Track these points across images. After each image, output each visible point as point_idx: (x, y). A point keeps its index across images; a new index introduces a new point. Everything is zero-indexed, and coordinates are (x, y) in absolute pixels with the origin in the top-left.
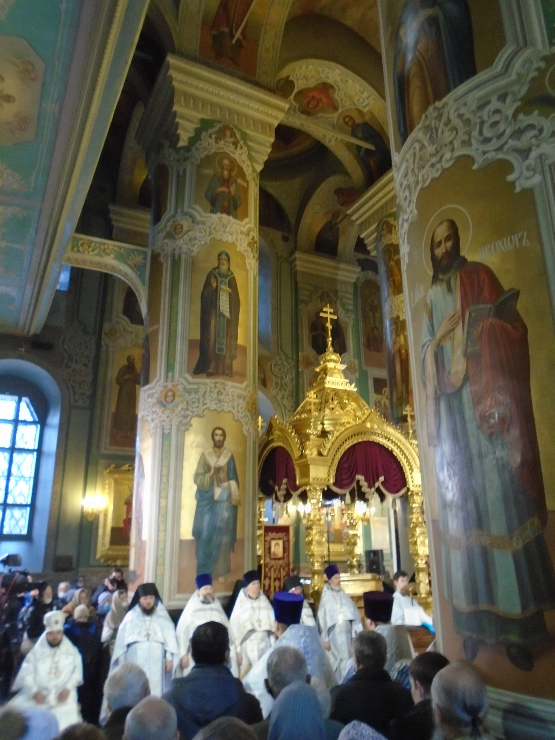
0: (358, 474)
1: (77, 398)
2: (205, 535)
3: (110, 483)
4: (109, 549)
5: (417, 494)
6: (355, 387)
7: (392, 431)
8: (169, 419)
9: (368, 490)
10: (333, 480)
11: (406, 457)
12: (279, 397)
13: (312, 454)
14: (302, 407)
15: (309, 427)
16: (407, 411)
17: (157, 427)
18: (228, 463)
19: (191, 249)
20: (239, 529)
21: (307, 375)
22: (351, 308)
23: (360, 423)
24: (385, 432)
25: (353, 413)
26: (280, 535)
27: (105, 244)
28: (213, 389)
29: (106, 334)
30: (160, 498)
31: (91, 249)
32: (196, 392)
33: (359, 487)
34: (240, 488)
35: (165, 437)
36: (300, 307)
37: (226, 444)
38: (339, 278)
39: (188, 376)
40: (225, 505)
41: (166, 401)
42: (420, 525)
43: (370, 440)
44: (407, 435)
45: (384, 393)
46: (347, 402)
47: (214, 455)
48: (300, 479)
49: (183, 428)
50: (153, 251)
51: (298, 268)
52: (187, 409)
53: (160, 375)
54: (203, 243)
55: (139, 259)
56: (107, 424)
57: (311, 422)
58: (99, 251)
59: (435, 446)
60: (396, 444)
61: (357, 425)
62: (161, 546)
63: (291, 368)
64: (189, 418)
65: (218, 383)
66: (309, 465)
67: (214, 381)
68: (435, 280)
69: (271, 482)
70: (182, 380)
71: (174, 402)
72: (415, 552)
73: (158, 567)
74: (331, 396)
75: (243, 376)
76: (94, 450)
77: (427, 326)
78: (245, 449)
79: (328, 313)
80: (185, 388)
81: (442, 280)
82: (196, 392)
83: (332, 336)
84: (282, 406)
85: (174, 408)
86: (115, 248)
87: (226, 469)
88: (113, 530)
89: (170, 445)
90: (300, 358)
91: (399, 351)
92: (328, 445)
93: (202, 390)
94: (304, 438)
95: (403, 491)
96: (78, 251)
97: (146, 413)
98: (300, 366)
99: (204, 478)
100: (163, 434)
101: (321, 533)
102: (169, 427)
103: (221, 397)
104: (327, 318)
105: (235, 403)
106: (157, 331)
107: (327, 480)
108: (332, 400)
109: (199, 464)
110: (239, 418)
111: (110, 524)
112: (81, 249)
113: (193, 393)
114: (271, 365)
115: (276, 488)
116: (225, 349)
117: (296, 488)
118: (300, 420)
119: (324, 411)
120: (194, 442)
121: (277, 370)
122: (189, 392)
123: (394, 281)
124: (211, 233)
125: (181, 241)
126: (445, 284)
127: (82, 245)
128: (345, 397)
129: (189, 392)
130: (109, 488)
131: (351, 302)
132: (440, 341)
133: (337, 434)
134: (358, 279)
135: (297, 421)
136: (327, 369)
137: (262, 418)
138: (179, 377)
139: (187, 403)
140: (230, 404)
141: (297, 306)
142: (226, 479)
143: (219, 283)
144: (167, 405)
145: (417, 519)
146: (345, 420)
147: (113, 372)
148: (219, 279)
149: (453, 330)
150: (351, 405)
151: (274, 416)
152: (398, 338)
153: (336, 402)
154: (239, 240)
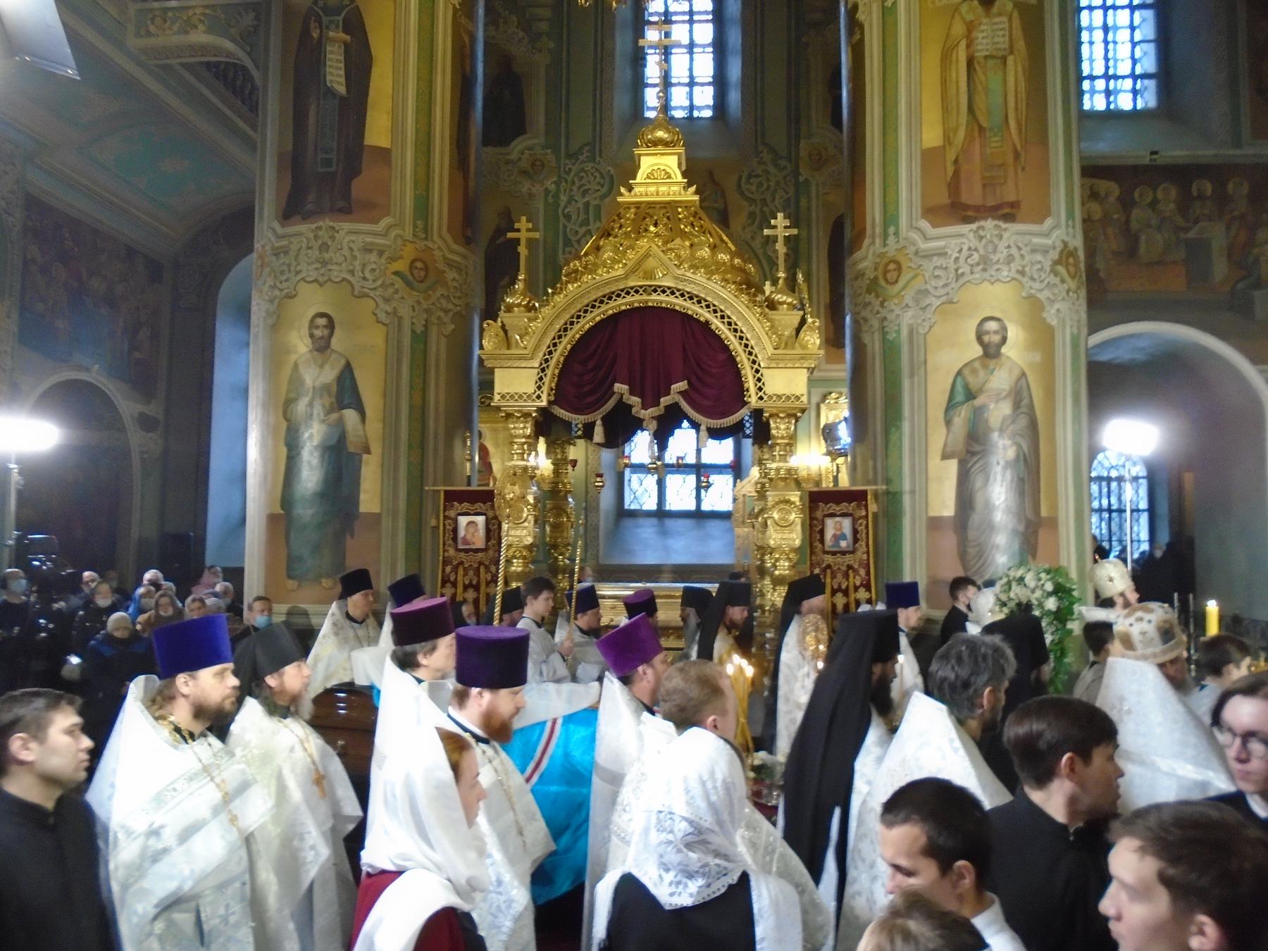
6: (696, 192)
9: (643, 411)
18: (340, 379)
21: (817, 185)
26: (479, 506)
31: (168, 24)
32: (286, 253)
33: (623, 409)
36: (804, 40)
37: (334, 342)
67: (313, 226)
82: (286, 253)
86: (207, 11)
87: (334, 388)
90: (801, 155)
93: (294, 248)
103: (327, 256)
105: (357, 263)
107: (534, 397)
112: (152, 29)
114: (740, 179)
116: (335, 160)
121: (753, 188)
140: (343, 265)
148: (325, 19)
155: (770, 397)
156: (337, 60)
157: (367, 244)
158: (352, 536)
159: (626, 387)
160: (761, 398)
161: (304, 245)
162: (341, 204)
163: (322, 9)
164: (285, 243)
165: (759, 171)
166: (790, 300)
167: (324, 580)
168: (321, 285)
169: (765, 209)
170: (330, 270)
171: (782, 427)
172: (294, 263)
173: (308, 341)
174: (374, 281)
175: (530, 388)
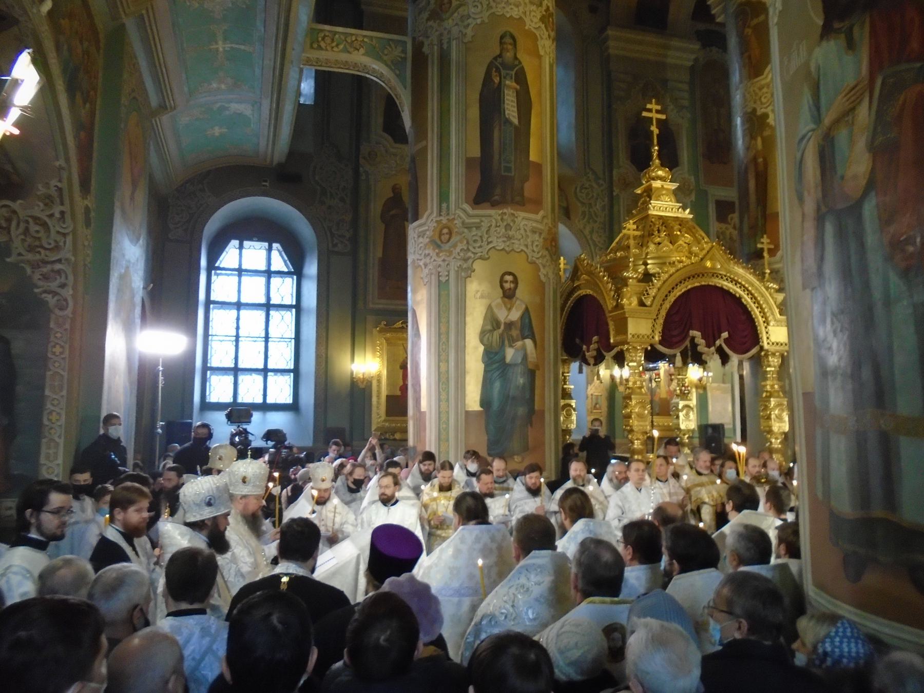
0: (693, 329)
1: (336, 241)
2: (496, 405)
3: (381, 344)
4: (385, 421)
5: (774, 354)
6: (690, 213)
7: (741, 272)
8: (446, 263)
9: (706, 349)
10: (659, 336)
11: (760, 306)
12: (587, 232)
13: (630, 304)
14: (617, 243)
15: (626, 268)
16: (764, 243)
17: (432, 274)
18: (522, 317)
19: (464, 31)
20: (537, 398)
22: (686, 103)
23: (696, 263)
24: (730, 272)
25: (687, 248)
27: (352, 35)
28: (500, 223)
29: (364, 158)
30: (439, 361)
31: (334, 44)
33: (694, 345)
34: (538, 346)
35: (442, 286)
38: (669, 61)
39: (466, 207)
40: (519, 370)
41: (441, 240)
42: (776, 394)
43: (710, 283)
44: (761, 276)
45: (729, 221)
46: (679, 233)
47: (504, 308)
48: (614, 337)
49: (463, 274)
50: (414, 39)
51: (611, 51)
52: (468, 249)
53: (432, 208)
54: (479, 21)
55: (397, 52)
56: (374, 273)
57: (630, 262)
58: (345, 45)
59: (813, 289)
60: (746, 289)
61: (693, 263)
62: (444, 419)
63: (602, 191)
64: (471, 261)
65: (505, 214)
66: (627, 318)
68: (827, 31)
69: (577, 341)
70: (459, 212)
71: (452, 240)
72: (768, 429)
73: (441, 443)
74: (657, 226)
75: (536, 204)
76: (360, 304)
77: (810, 108)
78: (543, 300)
79: (654, 111)
80: (463, 223)
81: (838, 31)
82: (478, 228)
83: (659, 144)
84: (590, 242)
85: (452, 249)
86: (366, 40)
88: (389, 398)
89: (448, 295)
90: (615, 178)
91: (755, 159)
92: (653, 292)
93: (485, 225)
94: (620, 283)
95: (754, 351)
96: (320, 48)
97: (418, 257)
98: (615, 189)
99: (492, 337)
100: (439, 281)
101: (642, 404)
102: (447, 273)
103: (511, 233)
104: (651, 119)
105: (529, 240)
106: (426, 148)
107: (651, 337)
108: (659, 231)
109: (485, 318)
110: (534, 259)
111: (384, 392)
112: (323, 44)
113: (475, 228)
114: (576, 188)
115: (584, 347)
117: (610, 348)
118: (615, 259)
119: (648, 247)
120: (477, 292)
122: (469, 227)
123: (749, 57)
124: (489, 7)
125: (450, 21)
126: (843, 36)
127: (323, 39)
128: (677, 227)
129: (469, 227)
130: (381, 349)
131: (686, 95)
132: (830, 129)
133: (664, 276)
134: (696, 60)
135: (610, 261)
136: (651, 190)
137: (564, 259)
138: (455, 210)
139: (468, 243)
140: (522, 240)
141: (609, 106)
142: (520, 337)
143: (502, 77)
144: (442, 245)
145: (772, 386)
146: (675, 258)
147: (376, 208)
148: (503, 72)
149: (853, 109)
150: (685, 237)
151: (581, 255)
152: (753, 142)
153: (663, 234)
154: (528, 13)
155: (773, 344)
156: (512, 101)
157: (533, 227)
158: (531, 425)
159: (700, 333)
160: (768, 344)
161: (494, 224)
162: (518, 198)
163: (500, 64)
164: (477, 220)
165: (587, 186)
166: (775, 286)
167: (516, 457)
168: (508, 253)
169: (591, 210)
170: (513, 243)
171: (776, 360)
172: (486, 236)
173: (500, 291)
174: (538, 253)
175: (649, 332)
